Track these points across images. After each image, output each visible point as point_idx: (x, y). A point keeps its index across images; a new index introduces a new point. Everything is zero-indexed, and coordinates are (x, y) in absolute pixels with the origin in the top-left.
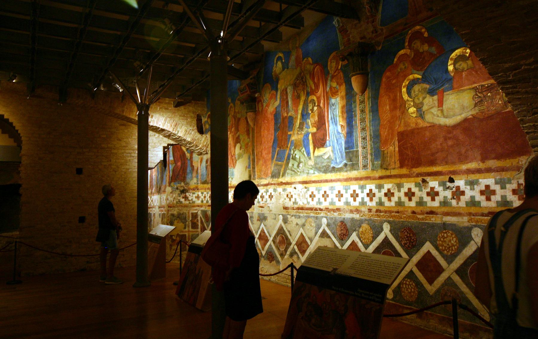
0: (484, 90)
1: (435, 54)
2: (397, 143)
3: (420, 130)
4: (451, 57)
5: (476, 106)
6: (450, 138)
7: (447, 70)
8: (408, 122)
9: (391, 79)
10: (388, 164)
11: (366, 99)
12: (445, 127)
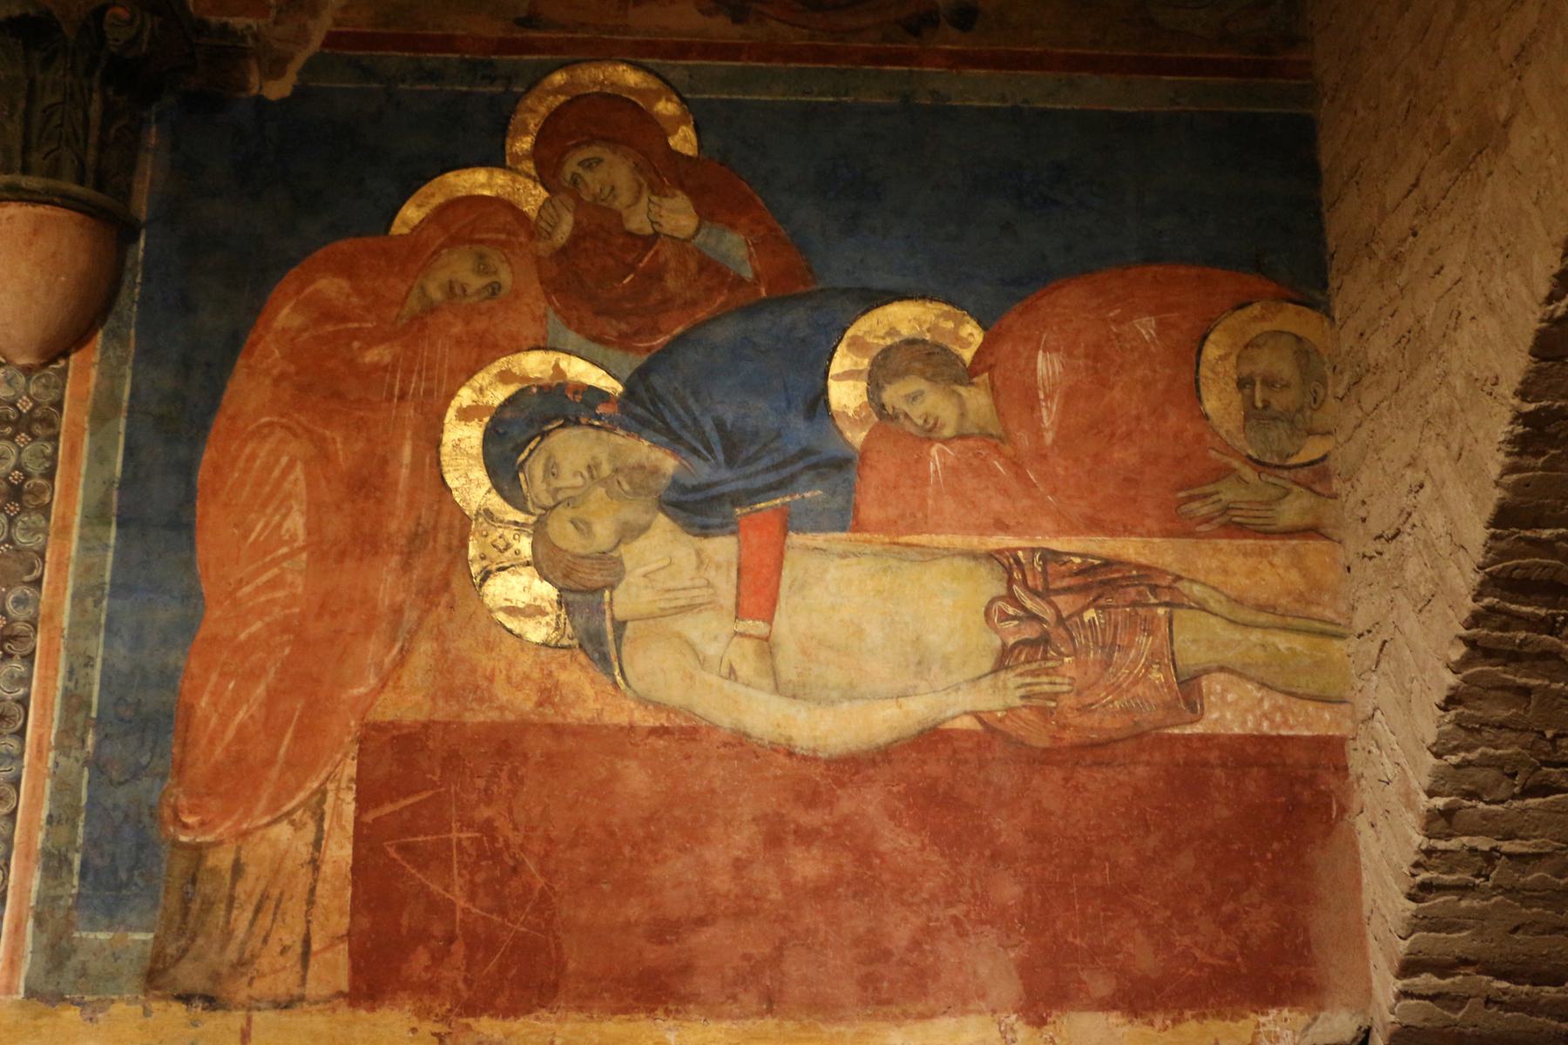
0: (1065, 583)
1: (740, 281)
2: (350, 809)
3: (570, 743)
4: (850, 333)
5: (1007, 668)
6: (806, 836)
7: (818, 403)
8: (473, 671)
9: (354, 335)
10: (231, 954)
11: (73, 415)
12: (782, 759)
